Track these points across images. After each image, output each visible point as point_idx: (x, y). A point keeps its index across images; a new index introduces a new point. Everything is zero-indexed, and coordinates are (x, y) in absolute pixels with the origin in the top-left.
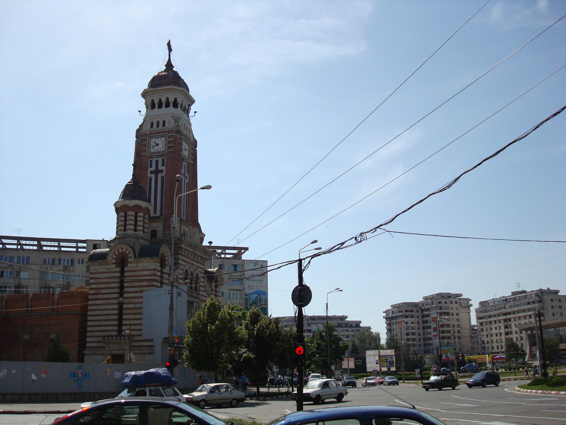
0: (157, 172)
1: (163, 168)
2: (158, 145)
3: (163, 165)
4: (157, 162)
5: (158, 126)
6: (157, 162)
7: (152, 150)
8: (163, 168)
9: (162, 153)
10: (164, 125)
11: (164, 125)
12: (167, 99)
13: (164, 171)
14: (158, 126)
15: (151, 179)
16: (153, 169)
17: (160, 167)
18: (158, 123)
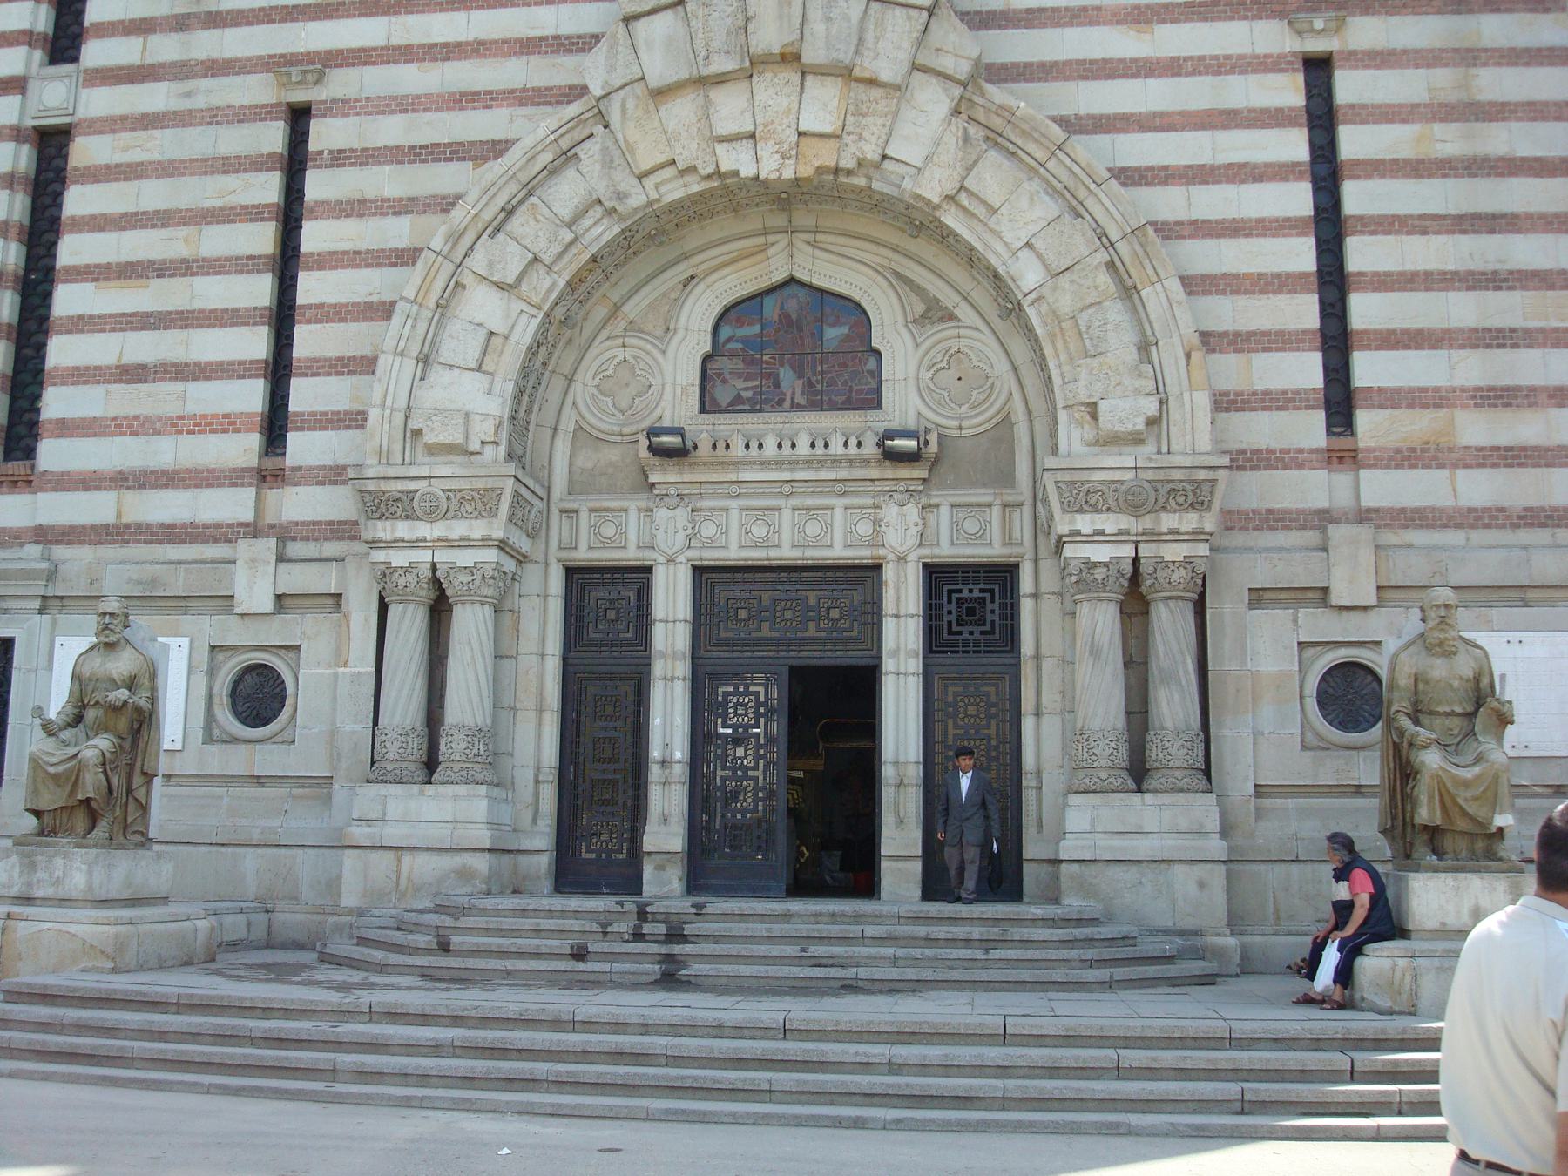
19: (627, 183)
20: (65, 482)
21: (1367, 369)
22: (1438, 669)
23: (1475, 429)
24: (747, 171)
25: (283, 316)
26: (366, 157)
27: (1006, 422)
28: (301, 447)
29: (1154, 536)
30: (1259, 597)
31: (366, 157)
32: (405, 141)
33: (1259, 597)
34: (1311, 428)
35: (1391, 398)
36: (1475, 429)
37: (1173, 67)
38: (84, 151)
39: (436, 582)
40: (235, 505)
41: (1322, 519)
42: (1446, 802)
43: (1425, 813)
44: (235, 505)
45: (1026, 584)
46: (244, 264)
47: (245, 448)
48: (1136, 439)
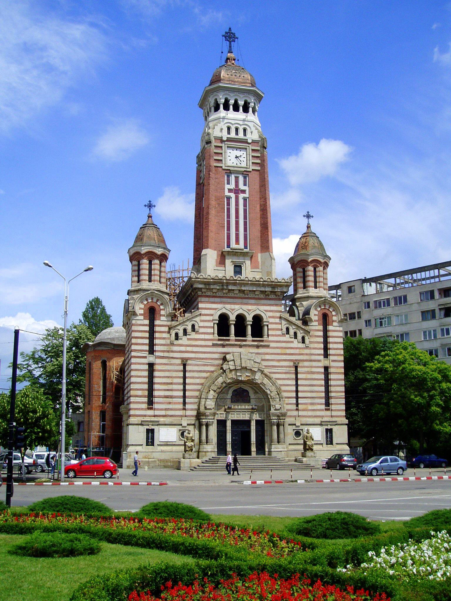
0: (237, 191)
1: (246, 188)
2: (237, 157)
3: (245, 185)
4: (237, 178)
5: (237, 133)
6: (237, 178)
7: (229, 163)
8: (246, 188)
9: (245, 169)
10: (245, 134)
11: (245, 134)
12: (236, 101)
13: (247, 192)
14: (237, 133)
15: (229, 198)
16: (232, 186)
17: (241, 187)
18: (237, 129)
19: (227, 379)
20: (158, 409)
21: (300, 401)
22: (308, 435)
23: (310, 407)
24: (240, 379)
25: (184, 390)
26: (193, 371)
27: (264, 405)
28: (187, 406)
29: (280, 419)
30: (289, 425)
31: (193, 371)
32: (198, 370)
33: (289, 425)
34: (294, 407)
35: (302, 404)
36: (310, 407)
37: (282, 367)
38: (156, 367)
39: (207, 423)
40: (181, 413)
41: (295, 416)
42: (309, 446)
43: (307, 448)
44: (181, 413)
45: (266, 422)
46: (179, 384)
47: (181, 406)
48: (279, 410)
